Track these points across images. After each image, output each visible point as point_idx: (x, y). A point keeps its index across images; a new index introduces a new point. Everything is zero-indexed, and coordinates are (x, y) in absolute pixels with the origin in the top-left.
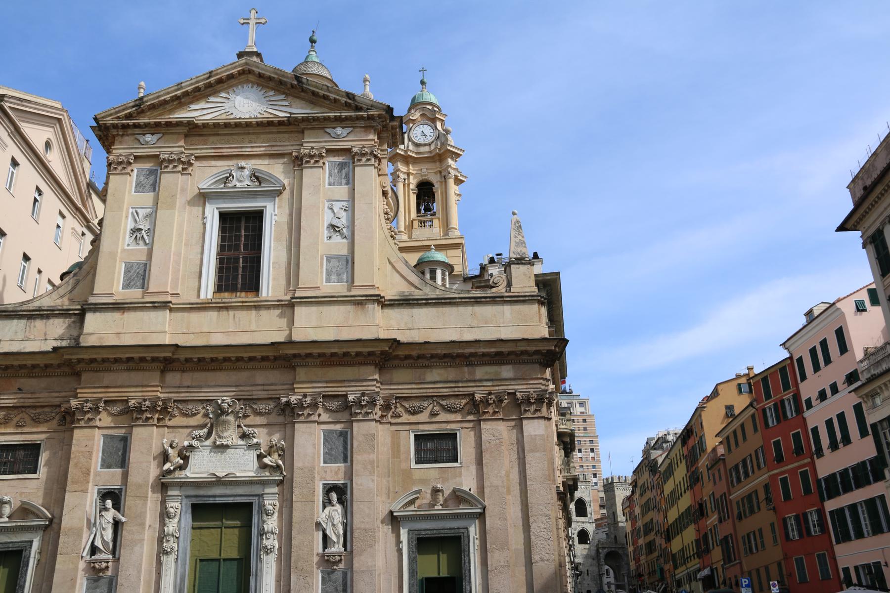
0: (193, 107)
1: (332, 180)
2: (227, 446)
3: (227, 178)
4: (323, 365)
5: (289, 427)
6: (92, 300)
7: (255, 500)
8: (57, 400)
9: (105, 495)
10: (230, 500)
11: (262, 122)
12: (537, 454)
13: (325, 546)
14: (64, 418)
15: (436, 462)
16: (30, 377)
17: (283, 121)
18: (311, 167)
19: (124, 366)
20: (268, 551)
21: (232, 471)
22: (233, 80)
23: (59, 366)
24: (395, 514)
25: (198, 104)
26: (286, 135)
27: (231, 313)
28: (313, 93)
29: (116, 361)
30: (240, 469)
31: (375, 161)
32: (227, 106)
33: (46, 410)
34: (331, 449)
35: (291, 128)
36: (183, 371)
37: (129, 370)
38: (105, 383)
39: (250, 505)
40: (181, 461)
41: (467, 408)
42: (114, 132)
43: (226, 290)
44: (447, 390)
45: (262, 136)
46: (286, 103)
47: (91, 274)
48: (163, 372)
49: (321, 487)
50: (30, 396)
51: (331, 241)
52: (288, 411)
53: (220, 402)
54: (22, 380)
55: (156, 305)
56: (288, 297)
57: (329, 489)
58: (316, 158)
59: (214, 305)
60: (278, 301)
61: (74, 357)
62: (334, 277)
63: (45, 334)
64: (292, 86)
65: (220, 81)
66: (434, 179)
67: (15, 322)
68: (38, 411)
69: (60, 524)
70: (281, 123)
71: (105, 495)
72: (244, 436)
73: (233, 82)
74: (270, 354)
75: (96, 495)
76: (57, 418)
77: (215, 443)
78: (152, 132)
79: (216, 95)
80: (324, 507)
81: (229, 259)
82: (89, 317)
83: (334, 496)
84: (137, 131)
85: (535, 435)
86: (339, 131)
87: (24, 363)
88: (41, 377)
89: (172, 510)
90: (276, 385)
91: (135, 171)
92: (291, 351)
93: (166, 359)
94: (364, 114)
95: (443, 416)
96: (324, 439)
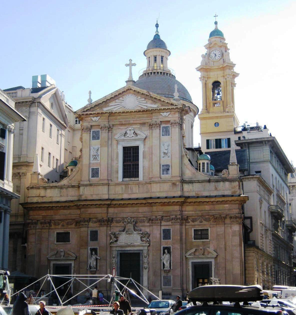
0: (110, 104)
1: (163, 133)
2: (130, 234)
3: (125, 134)
4: (161, 206)
5: (151, 228)
6: (82, 183)
7: (141, 252)
8: (74, 217)
9: (92, 250)
10: (133, 252)
11: (136, 111)
12: (236, 237)
13: (164, 268)
14: (76, 223)
15: (201, 239)
16: (64, 210)
17: (144, 111)
18: (155, 129)
19: (95, 206)
20: (146, 269)
21: (132, 242)
22: (125, 93)
23: (73, 206)
24: (187, 257)
25: (113, 103)
26: (146, 115)
27: (130, 186)
28: (155, 98)
29: (92, 205)
30: (136, 241)
31: (179, 126)
32: (123, 104)
33: (70, 221)
34: (165, 235)
35: (148, 112)
36: (114, 208)
37: (96, 208)
38: (89, 212)
39: (139, 253)
40: (116, 239)
41: (212, 220)
42: (83, 116)
43: (127, 177)
44: (205, 214)
45: (137, 116)
46: (145, 102)
47: (79, 172)
48: (108, 208)
49: (162, 248)
50: (65, 216)
51: (163, 158)
52: (150, 222)
53: (127, 219)
54: (62, 210)
55: (104, 184)
56: (150, 181)
57: (165, 248)
58: (158, 125)
59: (124, 184)
60: (146, 182)
61: (79, 204)
62: (165, 172)
63: (67, 195)
64: (147, 95)
65: (120, 94)
66: (221, 80)
67: (57, 190)
68: (69, 221)
69: (79, 259)
70: (143, 111)
71: (92, 250)
72: (135, 230)
73: (124, 93)
74: (144, 202)
75: (89, 250)
76: (74, 224)
77: (127, 232)
78: (96, 116)
79: (119, 99)
80: (163, 255)
81: (127, 165)
82: (81, 188)
83: (166, 251)
84: (91, 116)
85: (236, 230)
86: (165, 114)
87: (62, 205)
88: (67, 209)
89: (114, 255)
90: (146, 212)
91: (92, 132)
92: (150, 201)
93: (108, 204)
94: (175, 107)
95: (205, 222)
96: (163, 231)
